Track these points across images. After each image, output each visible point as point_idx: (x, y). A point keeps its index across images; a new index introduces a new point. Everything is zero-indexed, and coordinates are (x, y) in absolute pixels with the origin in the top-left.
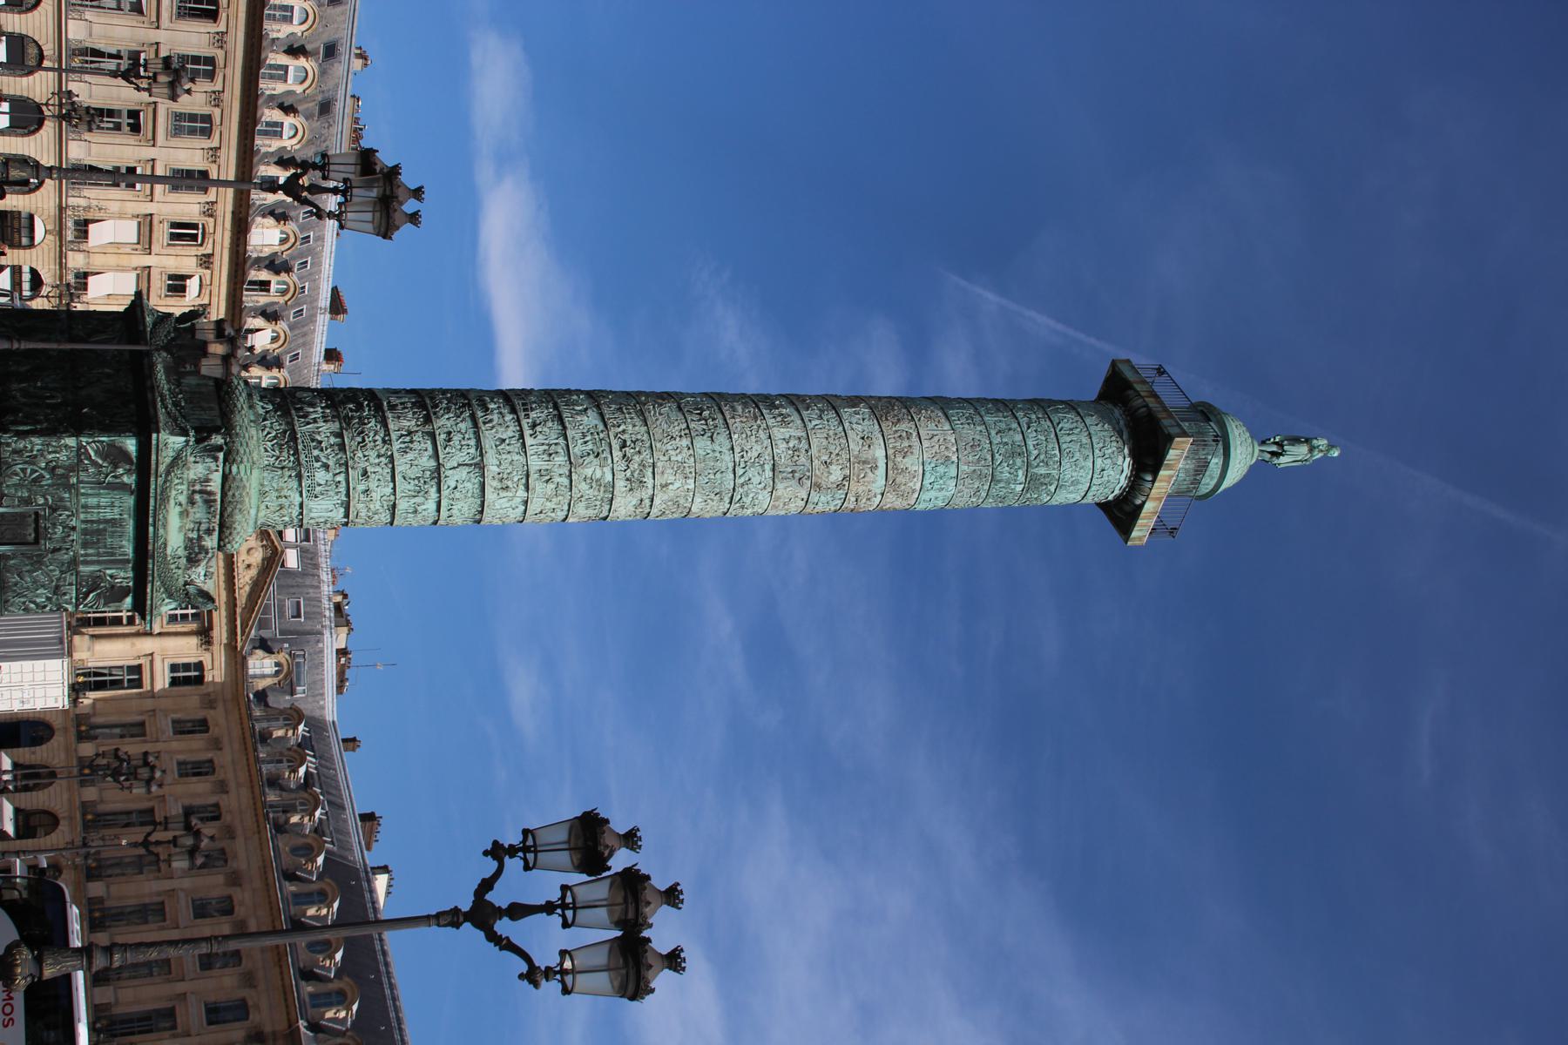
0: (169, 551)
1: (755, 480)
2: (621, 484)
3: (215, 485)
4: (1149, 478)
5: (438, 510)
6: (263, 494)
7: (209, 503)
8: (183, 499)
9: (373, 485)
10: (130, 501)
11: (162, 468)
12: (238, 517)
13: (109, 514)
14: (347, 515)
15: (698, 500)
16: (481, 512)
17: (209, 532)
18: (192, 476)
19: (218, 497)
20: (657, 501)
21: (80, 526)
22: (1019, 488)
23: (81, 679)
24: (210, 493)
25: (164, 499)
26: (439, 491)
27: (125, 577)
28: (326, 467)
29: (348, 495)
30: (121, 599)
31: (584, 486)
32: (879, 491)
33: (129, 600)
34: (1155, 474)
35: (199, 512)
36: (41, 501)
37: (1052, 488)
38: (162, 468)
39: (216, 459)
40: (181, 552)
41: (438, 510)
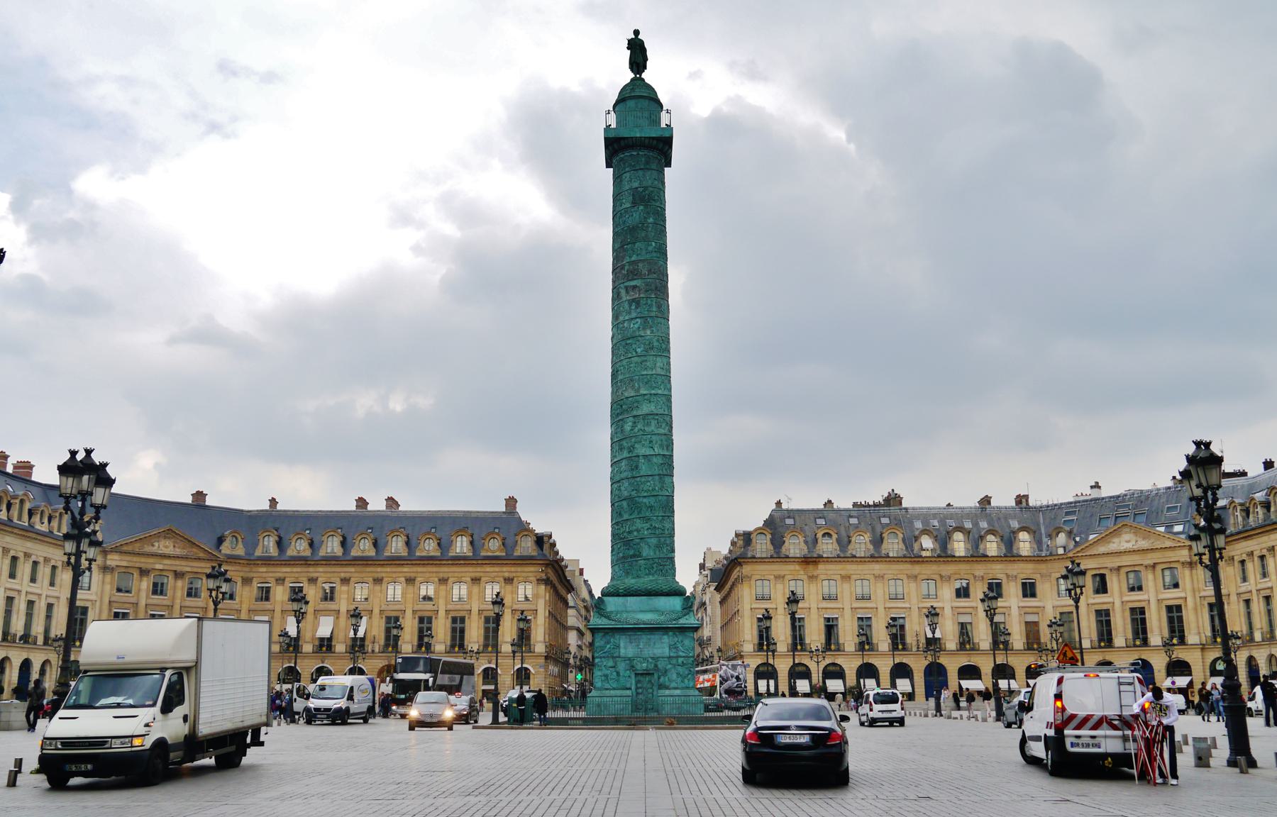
2: (635, 413)
23: (1219, 640)
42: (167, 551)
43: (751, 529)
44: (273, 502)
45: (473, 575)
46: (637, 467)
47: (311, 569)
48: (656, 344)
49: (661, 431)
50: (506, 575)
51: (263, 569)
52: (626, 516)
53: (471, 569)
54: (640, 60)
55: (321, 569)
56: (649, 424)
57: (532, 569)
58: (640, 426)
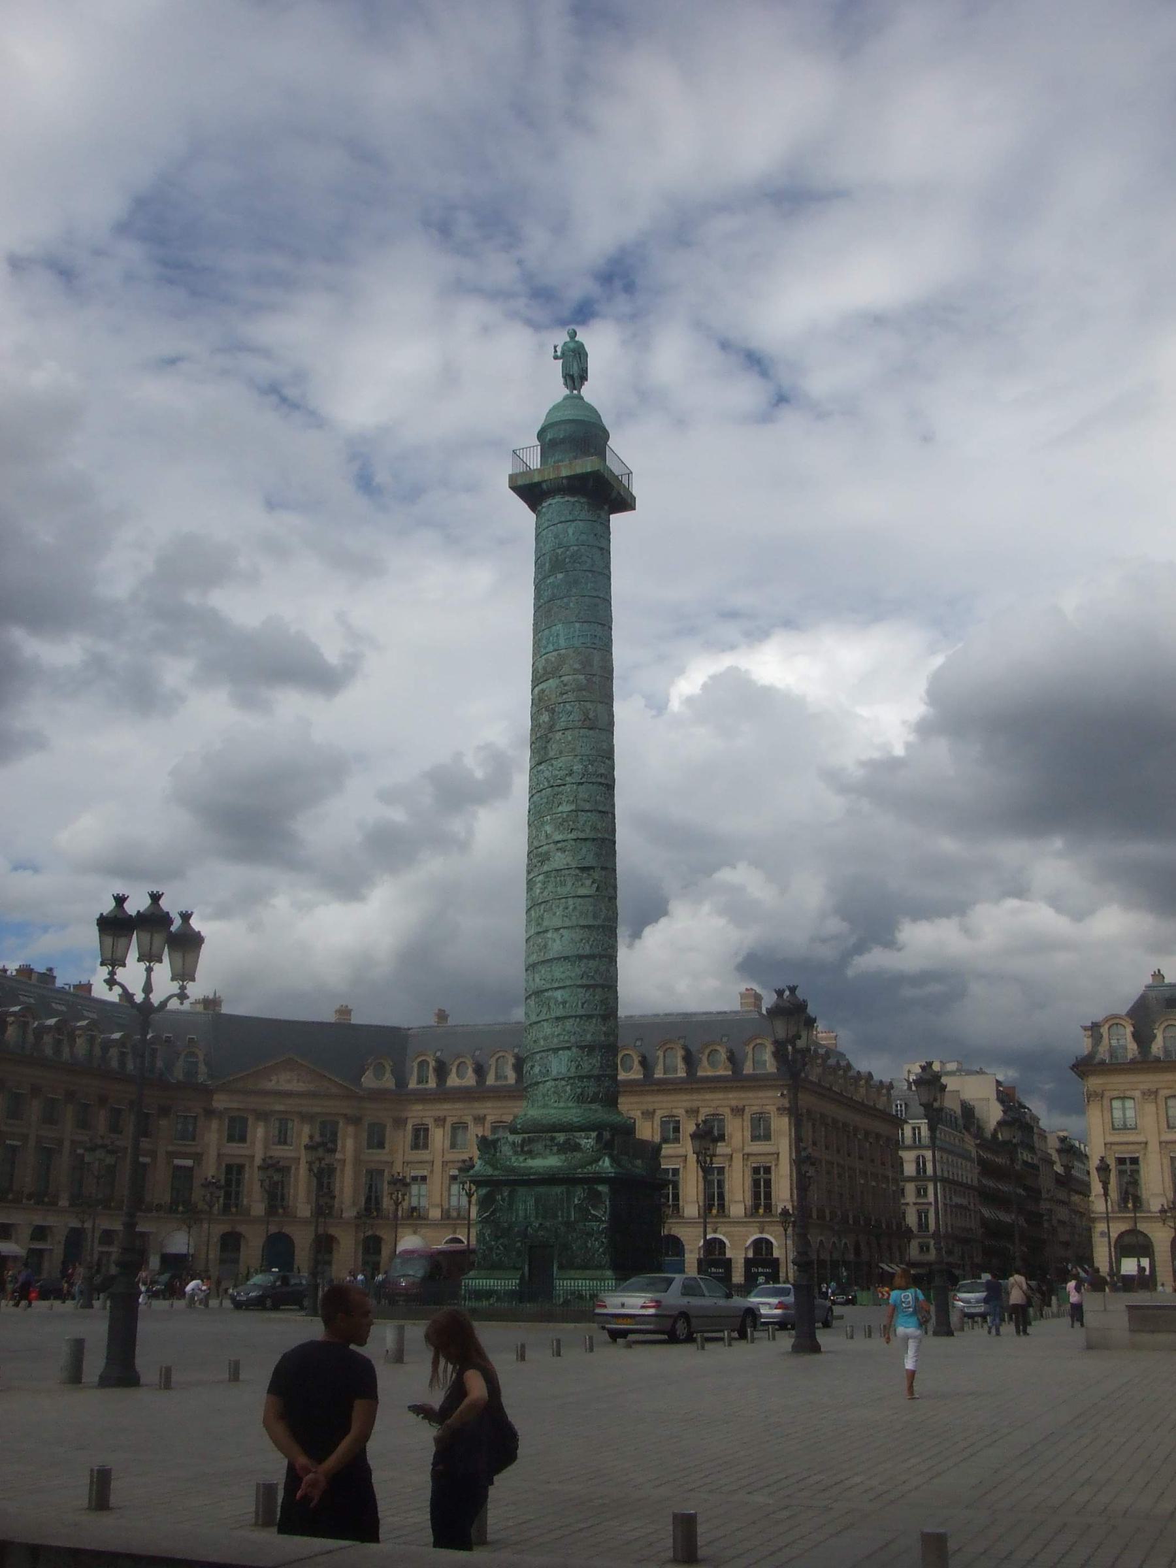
0: (559, 1164)
1: (547, 774)
2: (546, 868)
3: (518, 1139)
4: (544, 486)
5: (564, 987)
6: (545, 1106)
7: (531, 1141)
8: (521, 1159)
9: (541, 1035)
10: (521, 1191)
11: (490, 1171)
12: (544, 1122)
13: (531, 1202)
14: (569, 1048)
15: (560, 809)
16: (566, 958)
17: (553, 1139)
18: (510, 1153)
19: (526, 1136)
20: (559, 837)
21: (540, 1220)
22: (560, 576)
24: (524, 1140)
25: (513, 1170)
26: (547, 990)
27: (580, 1192)
28: (532, 1067)
29: (548, 1050)
30: (599, 1194)
31: (545, 893)
32: (558, 681)
33: (600, 1188)
34: (539, 484)
35: (538, 1147)
36: (519, 1244)
37: (559, 551)
38: (490, 1171)
39: (498, 1140)
40: (563, 1157)
41: (564, 987)
42: (288, 1087)
43: (1099, 1018)
44: (442, 1016)
45: (687, 1105)
46: (545, 946)
47: (476, 1105)
48: (577, 768)
49: (582, 891)
50: (734, 1103)
51: (420, 1107)
52: (534, 1018)
53: (685, 1097)
54: (575, 370)
55: (489, 1104)
56: (563, 884)
57: (770, 1094)
58: (550, 887)
